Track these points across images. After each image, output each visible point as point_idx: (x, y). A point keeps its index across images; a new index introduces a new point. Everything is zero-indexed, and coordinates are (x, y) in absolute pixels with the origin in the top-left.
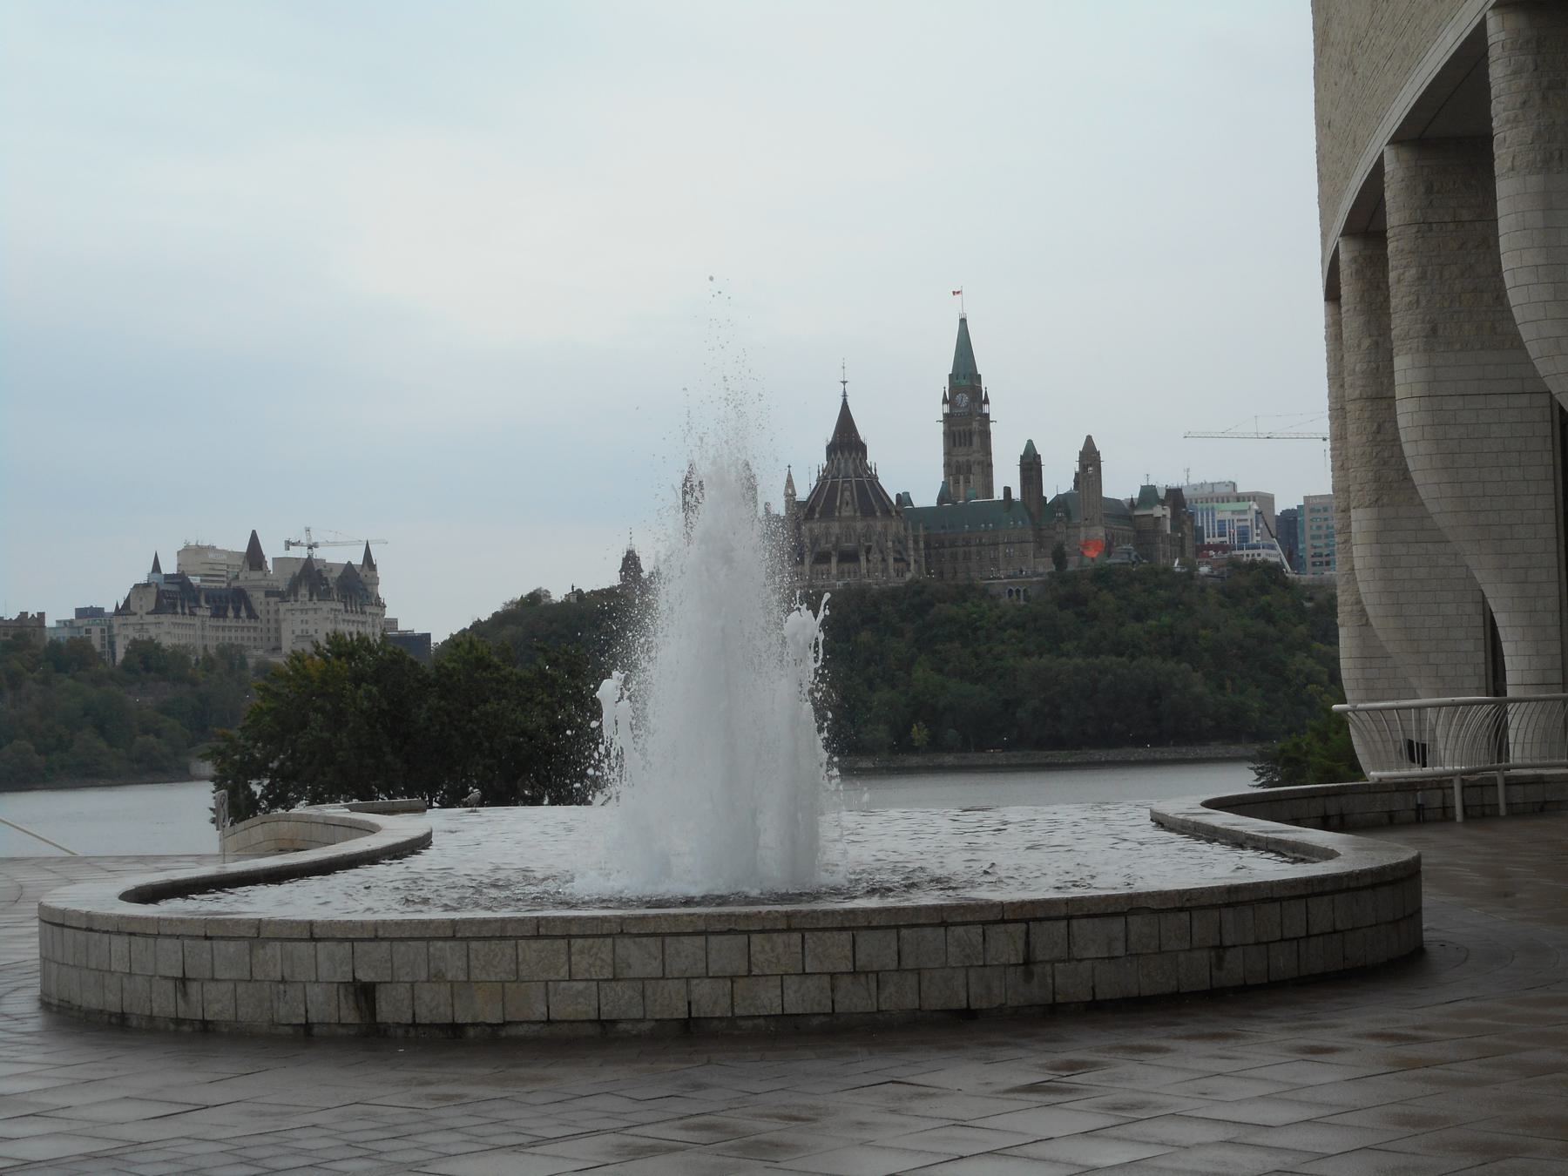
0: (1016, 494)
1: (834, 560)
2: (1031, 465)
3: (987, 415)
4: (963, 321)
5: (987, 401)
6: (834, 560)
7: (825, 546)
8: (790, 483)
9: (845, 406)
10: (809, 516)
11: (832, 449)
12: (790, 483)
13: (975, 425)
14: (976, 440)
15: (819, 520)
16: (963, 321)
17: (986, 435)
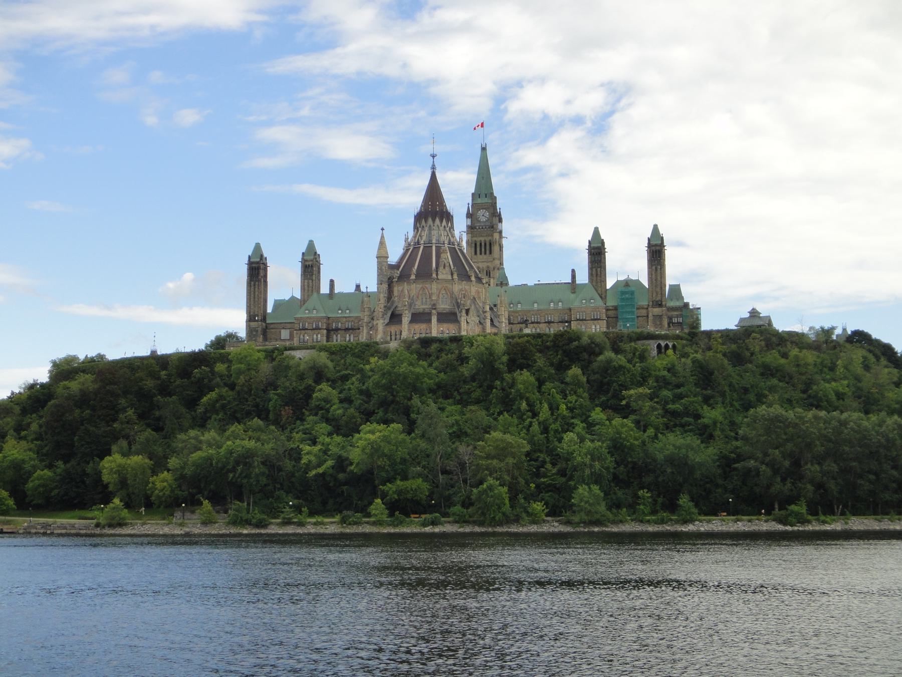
0: (583, 277)
1: (434, 319)
2: (597, 253)
3: (500, 232)
4: (484, 149)
5: (500, 220)
6: (434, 319)
7: (420, 306)
8: (382, 243)
9: (433, 178)
10: (404, 277)
11: (421, 217)
12: (382, 243)
13: (496, 236)
14: (496, 248)
15: (415, 281)
16: (484, 149)
17: (501, 247)
